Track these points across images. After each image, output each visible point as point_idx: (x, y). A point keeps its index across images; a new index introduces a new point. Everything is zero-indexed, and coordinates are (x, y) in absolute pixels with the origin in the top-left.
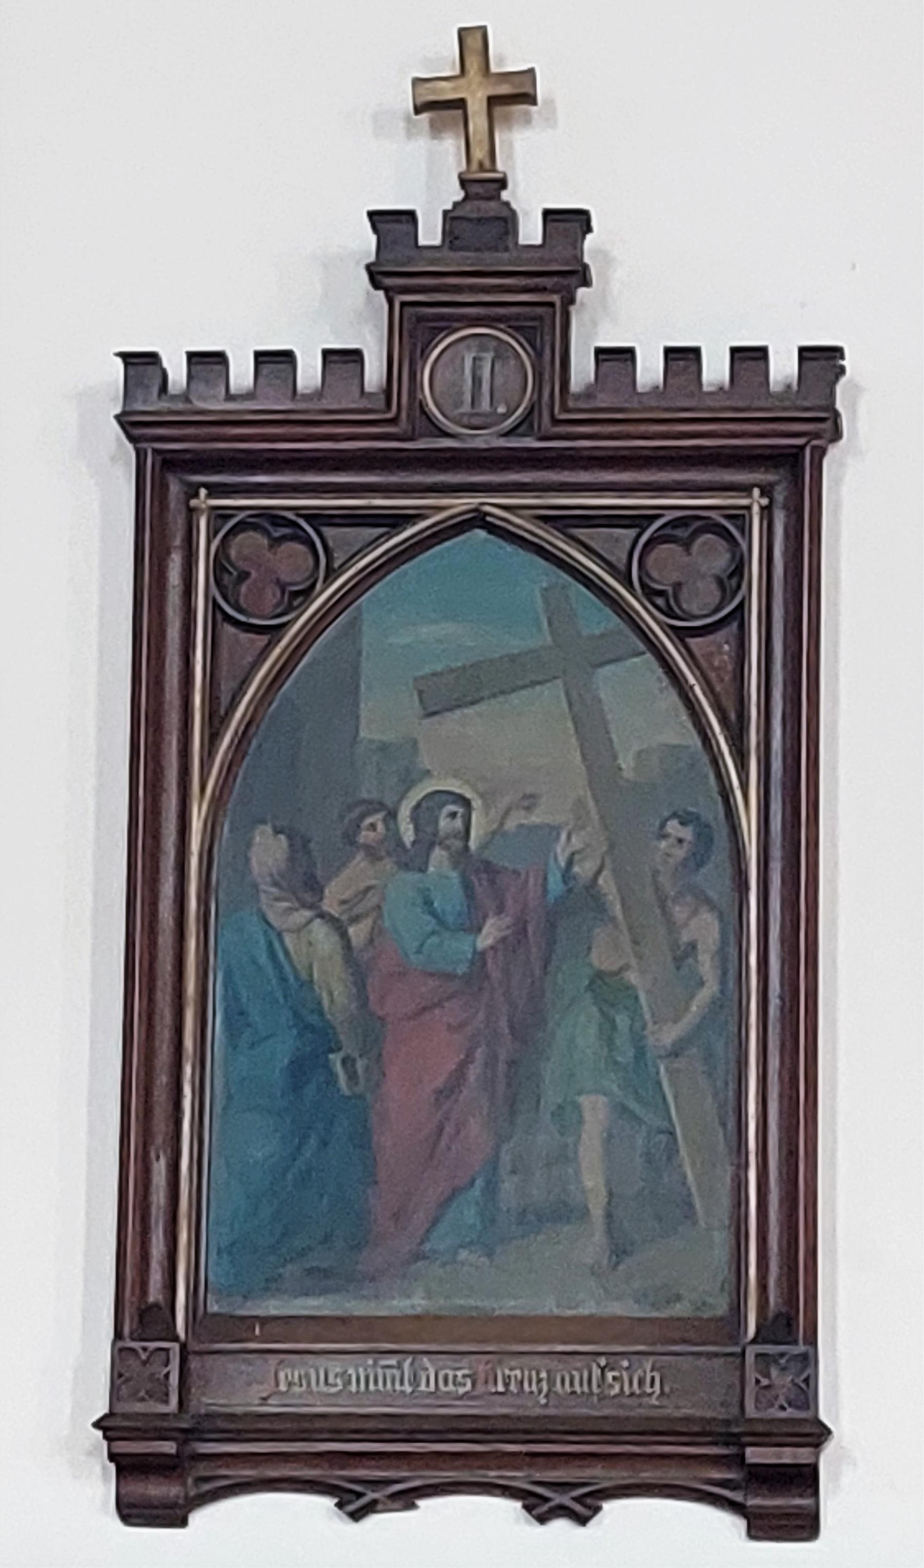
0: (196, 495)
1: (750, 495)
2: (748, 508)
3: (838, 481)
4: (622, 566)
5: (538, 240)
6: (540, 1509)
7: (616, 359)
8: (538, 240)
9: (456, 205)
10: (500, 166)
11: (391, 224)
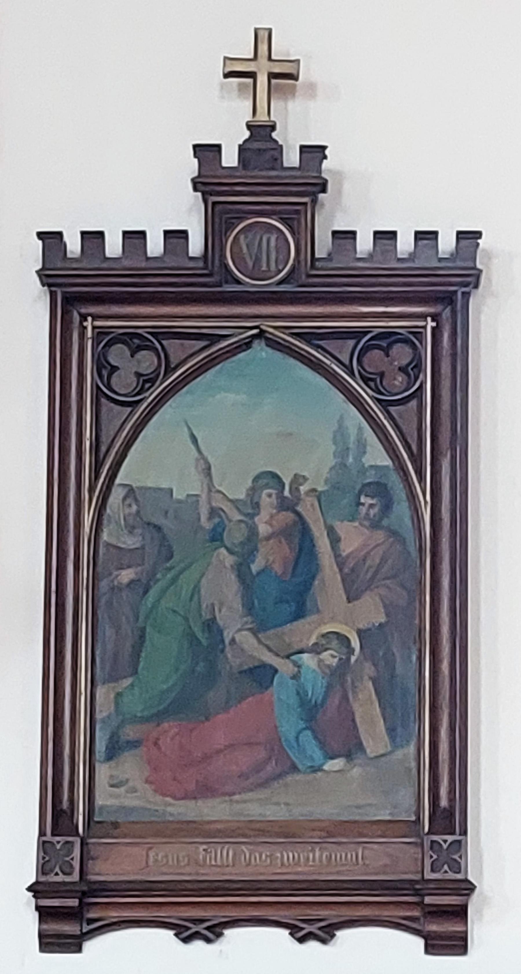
0: (86, 320)
1: (426, 320)
3: (479, 312)
4: (347, 362)
7: (346, 237)
8: (297, 164)
9: (246, 141)
11: (206, 152)
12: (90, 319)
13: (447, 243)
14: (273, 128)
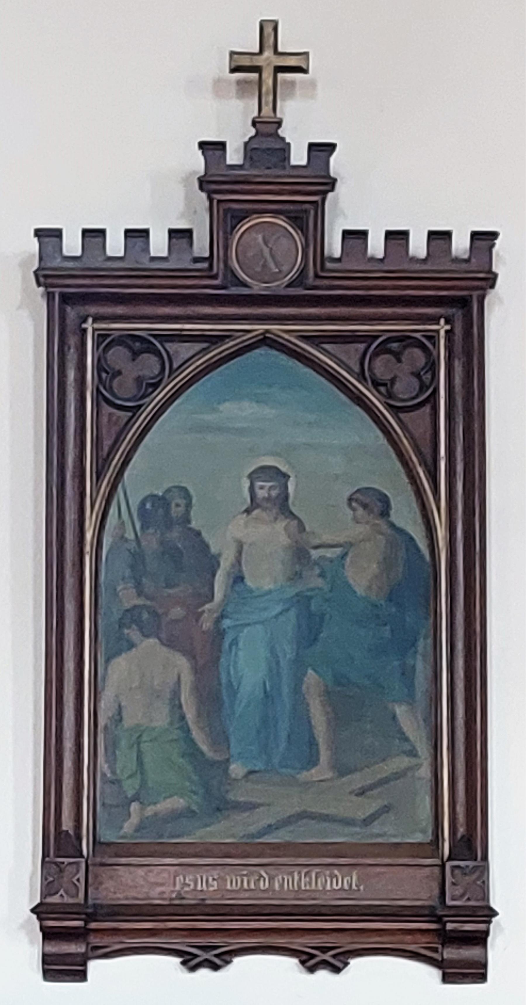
1: (438, 324)
2: (438, 331)
5: (304, 162)
6: (310, 963)
8: (304, 162)
10: (279, 115)
12: (90, 320)
13: (460, 244)
14: (279, 124)
